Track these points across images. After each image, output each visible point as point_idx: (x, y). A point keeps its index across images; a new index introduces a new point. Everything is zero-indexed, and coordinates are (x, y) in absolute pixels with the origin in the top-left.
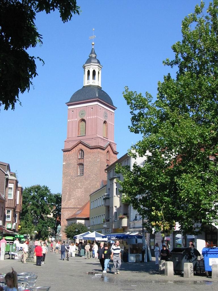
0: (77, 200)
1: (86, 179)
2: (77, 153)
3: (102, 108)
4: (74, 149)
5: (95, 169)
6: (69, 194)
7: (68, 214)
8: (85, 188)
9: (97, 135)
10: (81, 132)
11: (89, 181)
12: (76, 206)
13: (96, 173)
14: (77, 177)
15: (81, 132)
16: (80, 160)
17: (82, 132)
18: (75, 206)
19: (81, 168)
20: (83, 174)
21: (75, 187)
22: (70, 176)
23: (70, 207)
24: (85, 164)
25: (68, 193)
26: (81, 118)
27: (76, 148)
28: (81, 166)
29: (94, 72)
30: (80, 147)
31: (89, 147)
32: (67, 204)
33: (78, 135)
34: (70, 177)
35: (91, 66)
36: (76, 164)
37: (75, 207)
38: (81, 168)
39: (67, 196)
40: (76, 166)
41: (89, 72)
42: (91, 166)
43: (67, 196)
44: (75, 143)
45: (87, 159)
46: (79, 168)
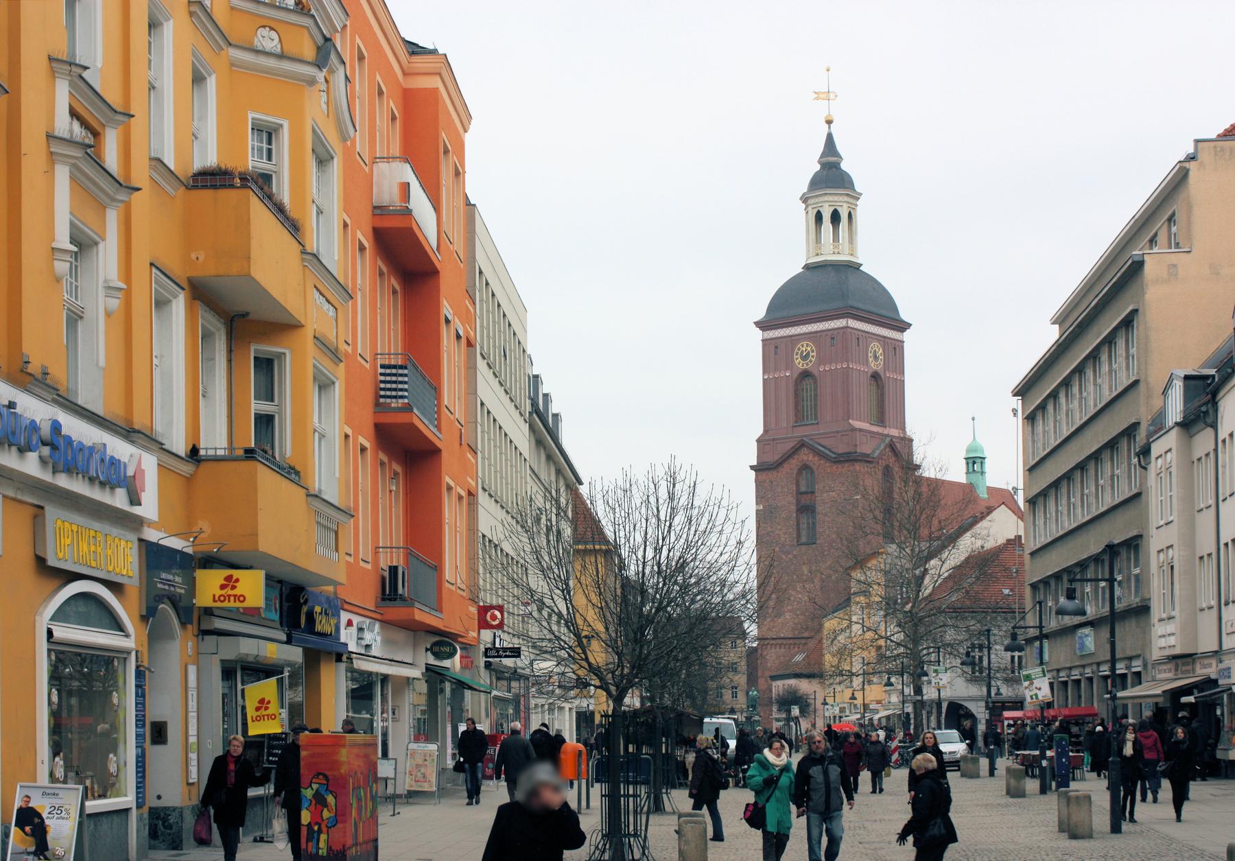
3: (864, 334)
4: (785, 465)
7: (778, 657)
9: (851, 421)
10: (803, 412)
17: (807, 411)
21: (795, 577)
23: (782, 635)
24: (819, 508)
30: (805, 458)
32: (773, 627)
33: (796, 422)
36: (793, 508)
40: (795, 515)
44: (788, 446)
45: (825, 495)
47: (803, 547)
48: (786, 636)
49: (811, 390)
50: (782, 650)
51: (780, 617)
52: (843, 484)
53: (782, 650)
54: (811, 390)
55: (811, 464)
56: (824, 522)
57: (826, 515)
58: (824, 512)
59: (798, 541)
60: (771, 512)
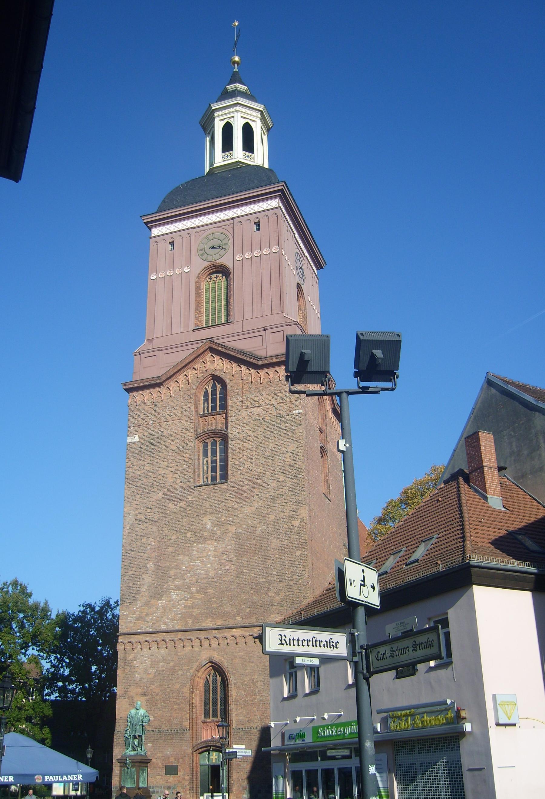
0: (198, 592)
1: (240, 497)
2: (193, 392)
4: (181, 378)
5: (284, 450)
6: (158, 567)
7: (154, 664)
8: (237, 537)
10: (207, 315)
11: (256, 505)
12: (196, 620)
13: (290, 466)
14: (196, 491)
15: (207, 315)
16: (210, 418)
18: (190, 621)
19: (214, 453)
20: (224, 477)
22: (159, 490)
23: (163, 627)
24: (233, 432)
25: (150, 565)
26: (207, 264)
27: (190, 372)
28: (214, 444)
29: (248, 130)
30: (209, 366)
31: (251, 360)
32: (147, 615)
34: (161, 495)
35: (238, 108)
36: (191, 435)
37: (187, 623)
38: (214, 453)
39: (147, 579)
40: (192, 444)
41: (228, 130)
42: (267, 438)
43: (147, 579)
44: (182, 355)
45: (244, 413)
46: (206, 454)
47: (206, 489)
48: (171, 628)
49: (220, 289)
50: (163, 651)
51: (160, 599)
52: (275, 395)
53: (163, 651)
54: (220, 289)
55: (222, 375)
56: (242, 450)
57: (245, 440)
58: (241, 436)
59: (195, 481)
60: (152, 444)
